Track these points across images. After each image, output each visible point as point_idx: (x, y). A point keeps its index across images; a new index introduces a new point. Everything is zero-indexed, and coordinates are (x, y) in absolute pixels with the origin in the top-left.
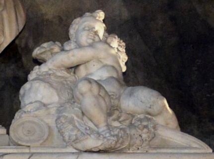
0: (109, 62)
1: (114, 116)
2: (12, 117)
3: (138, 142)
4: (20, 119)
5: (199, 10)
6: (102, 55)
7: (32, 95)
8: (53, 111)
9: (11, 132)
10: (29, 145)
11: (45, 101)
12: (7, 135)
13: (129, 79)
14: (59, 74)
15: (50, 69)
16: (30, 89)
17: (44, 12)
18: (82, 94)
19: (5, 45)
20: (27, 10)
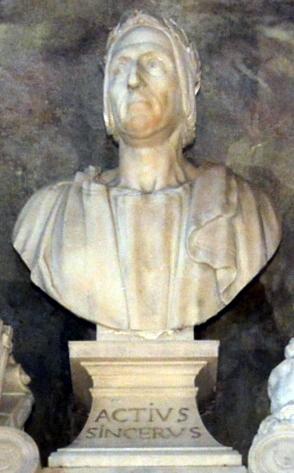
2: (253, 429)
4: (269, 434)
9: (251, 461)
12: (244, 467)
19: (240, 287)
20: (284, 216)
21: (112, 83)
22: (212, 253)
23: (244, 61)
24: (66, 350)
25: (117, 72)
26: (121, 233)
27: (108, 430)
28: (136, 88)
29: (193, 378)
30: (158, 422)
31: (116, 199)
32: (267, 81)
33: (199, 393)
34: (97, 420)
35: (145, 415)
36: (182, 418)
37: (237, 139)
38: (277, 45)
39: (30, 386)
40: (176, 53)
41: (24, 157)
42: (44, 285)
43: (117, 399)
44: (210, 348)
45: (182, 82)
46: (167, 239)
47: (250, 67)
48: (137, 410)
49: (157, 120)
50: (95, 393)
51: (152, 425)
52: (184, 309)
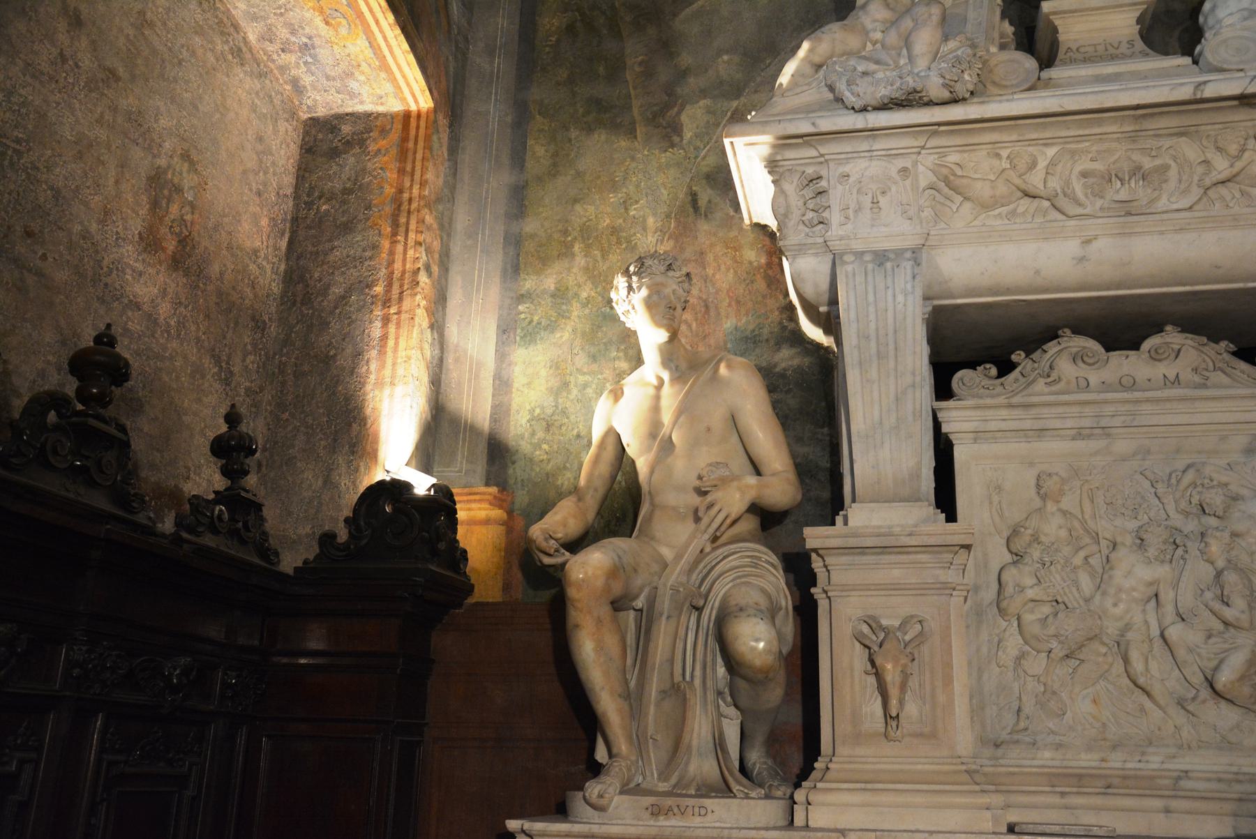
12: (1195, 66)
27: (1075, 59)
30: (1112, 51)
33: (1140, 29)
34: (1065, 54)
36: (1130, 46)
39: (1014, 34)
43: (1075, 40)
48: (1095, 45)
51: (1107, 53)
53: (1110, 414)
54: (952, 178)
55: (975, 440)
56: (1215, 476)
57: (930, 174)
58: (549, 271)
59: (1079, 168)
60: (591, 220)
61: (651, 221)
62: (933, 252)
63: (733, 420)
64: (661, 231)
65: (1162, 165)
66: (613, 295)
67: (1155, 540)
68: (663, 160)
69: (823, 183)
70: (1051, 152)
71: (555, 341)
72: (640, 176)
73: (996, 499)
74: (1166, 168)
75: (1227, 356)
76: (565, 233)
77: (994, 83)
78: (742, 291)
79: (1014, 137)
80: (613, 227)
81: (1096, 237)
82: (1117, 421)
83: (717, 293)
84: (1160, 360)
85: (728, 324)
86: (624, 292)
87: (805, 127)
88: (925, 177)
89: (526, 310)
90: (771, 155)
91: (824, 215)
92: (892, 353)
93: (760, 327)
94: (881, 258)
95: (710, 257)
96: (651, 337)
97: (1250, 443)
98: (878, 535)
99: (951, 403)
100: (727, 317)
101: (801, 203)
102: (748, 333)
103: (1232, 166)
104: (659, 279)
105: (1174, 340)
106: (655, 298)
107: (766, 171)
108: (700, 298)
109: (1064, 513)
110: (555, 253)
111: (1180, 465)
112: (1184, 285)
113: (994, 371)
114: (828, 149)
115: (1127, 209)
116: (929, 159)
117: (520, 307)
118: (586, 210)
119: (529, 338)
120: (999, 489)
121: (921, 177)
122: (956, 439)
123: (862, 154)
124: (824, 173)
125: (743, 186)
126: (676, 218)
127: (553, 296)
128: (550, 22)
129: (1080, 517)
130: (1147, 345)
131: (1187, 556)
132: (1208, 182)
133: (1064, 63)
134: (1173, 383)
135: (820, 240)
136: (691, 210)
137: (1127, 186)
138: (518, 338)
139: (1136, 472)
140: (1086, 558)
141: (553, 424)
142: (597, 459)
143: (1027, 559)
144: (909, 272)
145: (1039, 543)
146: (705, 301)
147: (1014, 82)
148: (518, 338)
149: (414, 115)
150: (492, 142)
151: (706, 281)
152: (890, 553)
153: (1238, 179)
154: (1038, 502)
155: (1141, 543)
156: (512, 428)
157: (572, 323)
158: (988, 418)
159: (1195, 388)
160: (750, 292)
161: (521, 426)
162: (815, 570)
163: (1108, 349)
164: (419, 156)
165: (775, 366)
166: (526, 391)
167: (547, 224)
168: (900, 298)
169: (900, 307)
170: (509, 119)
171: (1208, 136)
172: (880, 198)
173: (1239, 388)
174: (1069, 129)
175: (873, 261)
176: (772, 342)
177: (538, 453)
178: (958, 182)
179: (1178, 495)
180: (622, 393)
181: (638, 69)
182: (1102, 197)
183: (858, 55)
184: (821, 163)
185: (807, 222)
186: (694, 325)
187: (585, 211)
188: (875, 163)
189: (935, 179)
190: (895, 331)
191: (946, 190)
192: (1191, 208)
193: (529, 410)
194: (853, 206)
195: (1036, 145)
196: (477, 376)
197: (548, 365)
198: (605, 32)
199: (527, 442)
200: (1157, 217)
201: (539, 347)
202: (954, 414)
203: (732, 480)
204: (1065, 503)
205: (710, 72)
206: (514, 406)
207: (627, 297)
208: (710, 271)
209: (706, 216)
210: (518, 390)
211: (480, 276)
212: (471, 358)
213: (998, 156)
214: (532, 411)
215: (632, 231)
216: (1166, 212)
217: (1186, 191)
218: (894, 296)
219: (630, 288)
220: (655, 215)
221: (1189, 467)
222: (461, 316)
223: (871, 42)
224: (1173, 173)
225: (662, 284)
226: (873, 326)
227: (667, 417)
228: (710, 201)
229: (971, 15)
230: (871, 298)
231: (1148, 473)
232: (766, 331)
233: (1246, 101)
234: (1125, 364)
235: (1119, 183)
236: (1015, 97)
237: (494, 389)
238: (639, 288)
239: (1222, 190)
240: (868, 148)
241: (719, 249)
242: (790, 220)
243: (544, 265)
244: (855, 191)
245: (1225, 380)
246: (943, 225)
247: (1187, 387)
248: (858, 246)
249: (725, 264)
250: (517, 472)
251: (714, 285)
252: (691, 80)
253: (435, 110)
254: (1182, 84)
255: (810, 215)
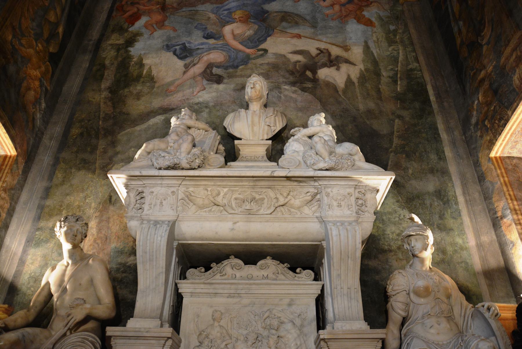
0: (329, 133)
1: (333, 155)
3: (346, 166)
5: (368, 122)
6: (325, 130)
7: (290, 147)
8: (301, 154)
10: (289, 168)
11: (297, 150)
13: (339, 141)
14: (304, 139)
15: (299, 137)
16: (289, 145)
17: (295, 123)
18: (316, 143)
21: (247, 89)
22: (270, 123)
23: (278, 92)
24: (234, 142)
25: (249, 86)
26: (248, 119)
28: (253, 88)
29: (265, 150)
30: (256, 159)
31: (247, 112)
32: (284, 96)
35: (253, 157)
37: (277, 107)
38: (285, 89)
40: (262, 82)
41: (227, 109)
42: (230, 131)
43: (245, 154)
44: (270, 142)
45: (264, 88)
46: (259, 120)
47: (279, 93)
49: (258, 95)
50: (241, 153)
52: (263, 135)
53: (241, 288)
54: (189, 196)
55: (191, 296)
56: (276, 314)
57: (183, 194)
58: (51, 220)
59: (234, 197)
60: (71, 202)
61: (93, 204)
62: (180, 223)
63: (91, 281)
64: (96, 208)
65: (262, 198)
66: (55, 229)
67: (252, 338)
68: (103, 183)
69: (144, 194)
70: (226, 190)
71: (46, 247)
72: (93, 188)
73: (196, 320)
74: (263, 199)
75: (286, 269)
76: (61, 206)
77: (209, 164)
78: (120, 233)
79: (212, 184)
80: (79, 206)
81: (238, 222)
82: (243, 291)
83: (111, 233)
84: (262, 269)
85: (113, 245)
86: (58, 227)
87: (137, 173)
88: (181, 195)
89: (39, 234)
90: (126, 182)
91: (142, 206)
92: (155, 259)
93: (125, 247)
94: (156, 223)
95: (111, 220)
96: (67, 247)
97: (290, 302)
98: (135, 331)
99: (182, 281)
100: (113, 243)
101: (135, 201)
102: (120, 250)
103: (284, 200)
104: (72, 224)
105: (269, 262)
106: (69, 231)
107: (124, 188)
108: (105, 235)
109: (221, 326)
110: (55, 213)
111: (265, 309)
112: (269, 242)
113: (203, 270)
114: (147, 182)
115: (249, 212)
116: (182, 189)
117: (37, 233)
118: (71, 198)
119: (37, 245)
120: (198, 316)
121: (179, 195)
122: (185, 295)
123: (159, 185)
124: (145, 191)
125: (121, 193)
126: (102, 204)
127: (50, 229)
128: (75, 131)
129: (227, 329)
130: (259, 263)
131: (262, 345)
132: (276, 205)
133: (239, 161)
134: (265, 278)
135: (139, 215)
136: (109, 202)
137: (249, 204)
138: (33, 245)
139: (249, 311)
140: (226, 345)
141: (38, 280)
142: (40, 293)
143: (203, 345)
144: (165, 229)
145: (208, 338)
146: (106, 236)
147: (215, 165)
148: (33, 245)
149: (8, 157)
150: (43, 170)
151: (108, 229)
152: (140, 339)
153: (287, 205)
154: (212, 322)
155: (246, 340)
156: (21, 280)
157: (55, 241)
158: (196, 288)
159: (273, 280)
160: (123, 234)
161: (25, 280)
162: (112, 345)
163: (246, 264)
164: (6, 172)
165: (127, 263)
166: (30, 266)
167: (55, 202)
168: (159, 238)
169: (159, 241)
170: (51, 163)
171: (278, 189)
172: (163, 201)
173: (288, 281)
174: (231, 182)
175: (153, 224)
176: (128, 254)
177: (28, 291)
178: (191, 198)
179: (262, 321)
180: (55, 268)
181: (101, 150)
182: (241, 208)
183: (164, 151)
184: (144, 187)
185: (136, 208)
186: (100, 245)
187: (70, 199)
188: (163, 189)
189: (184, 196)
190: (156, 251)
191: (188, 200)
192: (271, 214)
193: (30, 274)
194: (153, 203)
195: (220, 187)
196: (13, 259)
197: (42, 256)
198: (94, 136)
199: (26, 287)
200: (259, 216)
201: (40, 249)
202: (184, 285)
203: (80, 305)
204: (222, 323)
205: (126, 154)
206: (24, 271)
207: (60, 230)
208: (110, 225)
209: (113, 204)
210: (27, 265)
211: (24, 220)
212: (13, 251)
213: (207, 190)
214: (30, 274)
215: (86, 208)
216: (263, 214)
217: (269, 208)
218: (157, 237)
219: (61, 227)
220: (95, 202)
221: (268, 310)
222: (13, 234)
223: (170, 146)
224: (266, 201)
225: (73, 226)
226: (148, 248)
227: (66, 279)
228: (116, 199)
229: (207, 141)
230: (149, 238)
231: (253, 312)
232: (126, 249)
233: (288, 179)
234: (251, 270)
235: (247, 203)
236: (214, 169)
237: (18, 264)
238: (64, 227)
239: (281, 208)
240: (161, 183)
241: (116, 217)
242: (130, 207)
243: (50, 217)
244: (155, 198)
245: (282, 277)
246: (185, 213)
247: (270, 280)
248: (152, 218)
249: (117, 223)
250: (18, 299)
251: (111, 230)
252: (119, 156)
253: (17, 156)
254: (268, 171)
255: (138, 205)
